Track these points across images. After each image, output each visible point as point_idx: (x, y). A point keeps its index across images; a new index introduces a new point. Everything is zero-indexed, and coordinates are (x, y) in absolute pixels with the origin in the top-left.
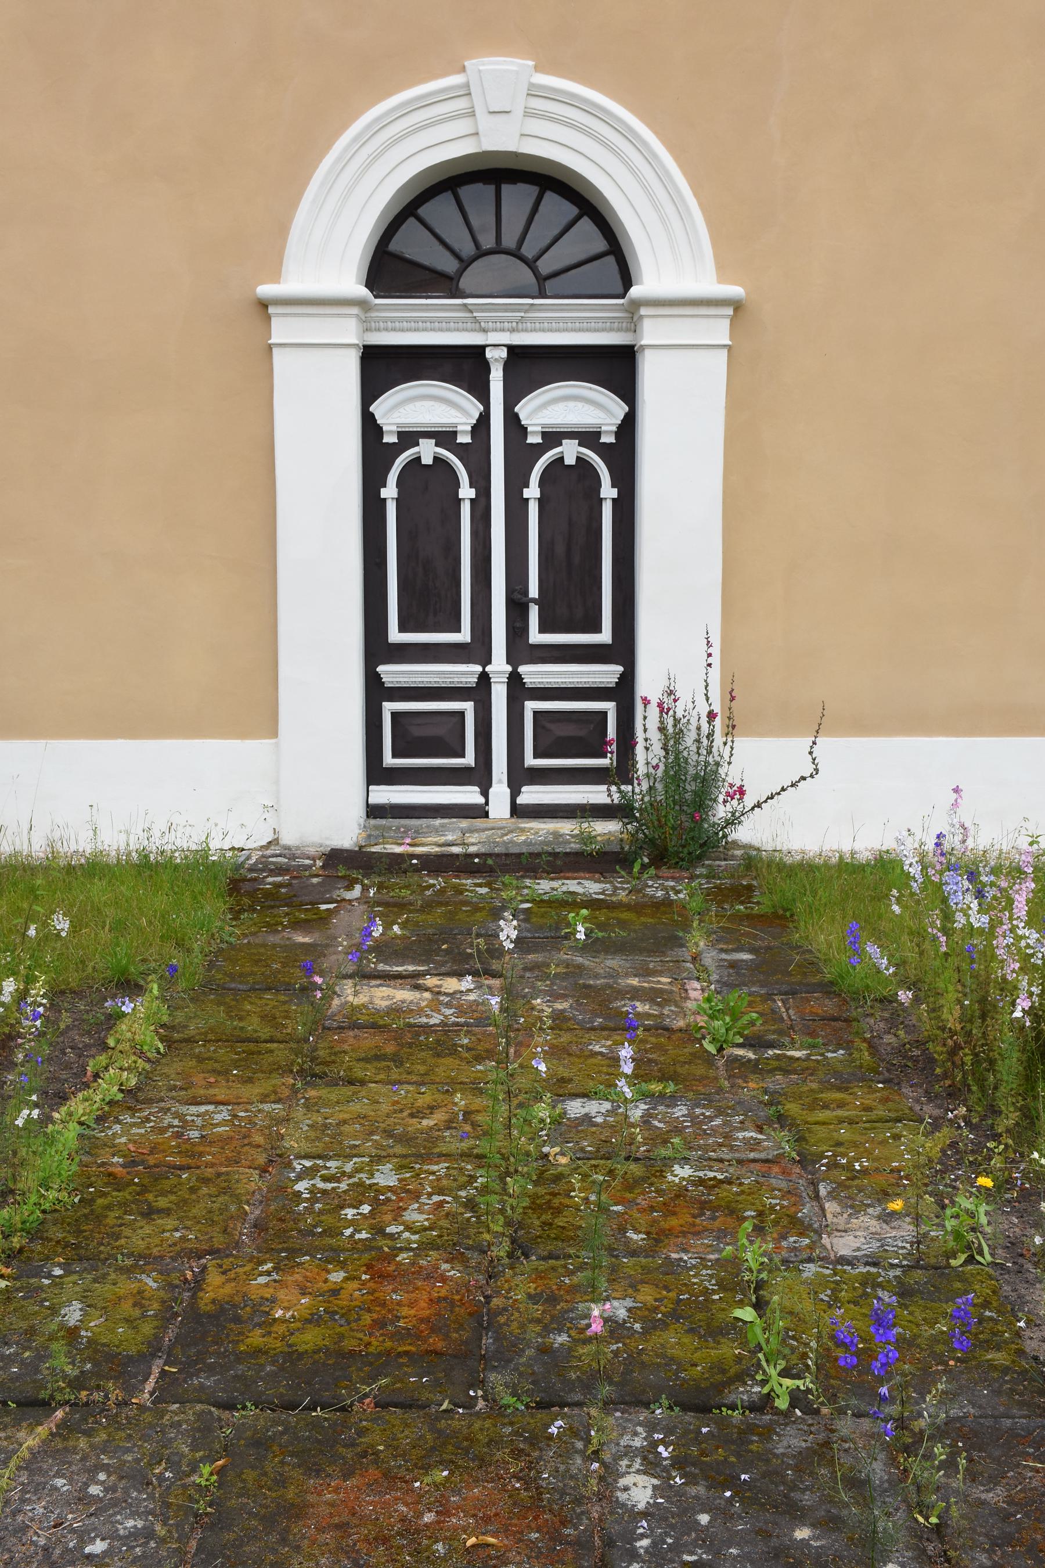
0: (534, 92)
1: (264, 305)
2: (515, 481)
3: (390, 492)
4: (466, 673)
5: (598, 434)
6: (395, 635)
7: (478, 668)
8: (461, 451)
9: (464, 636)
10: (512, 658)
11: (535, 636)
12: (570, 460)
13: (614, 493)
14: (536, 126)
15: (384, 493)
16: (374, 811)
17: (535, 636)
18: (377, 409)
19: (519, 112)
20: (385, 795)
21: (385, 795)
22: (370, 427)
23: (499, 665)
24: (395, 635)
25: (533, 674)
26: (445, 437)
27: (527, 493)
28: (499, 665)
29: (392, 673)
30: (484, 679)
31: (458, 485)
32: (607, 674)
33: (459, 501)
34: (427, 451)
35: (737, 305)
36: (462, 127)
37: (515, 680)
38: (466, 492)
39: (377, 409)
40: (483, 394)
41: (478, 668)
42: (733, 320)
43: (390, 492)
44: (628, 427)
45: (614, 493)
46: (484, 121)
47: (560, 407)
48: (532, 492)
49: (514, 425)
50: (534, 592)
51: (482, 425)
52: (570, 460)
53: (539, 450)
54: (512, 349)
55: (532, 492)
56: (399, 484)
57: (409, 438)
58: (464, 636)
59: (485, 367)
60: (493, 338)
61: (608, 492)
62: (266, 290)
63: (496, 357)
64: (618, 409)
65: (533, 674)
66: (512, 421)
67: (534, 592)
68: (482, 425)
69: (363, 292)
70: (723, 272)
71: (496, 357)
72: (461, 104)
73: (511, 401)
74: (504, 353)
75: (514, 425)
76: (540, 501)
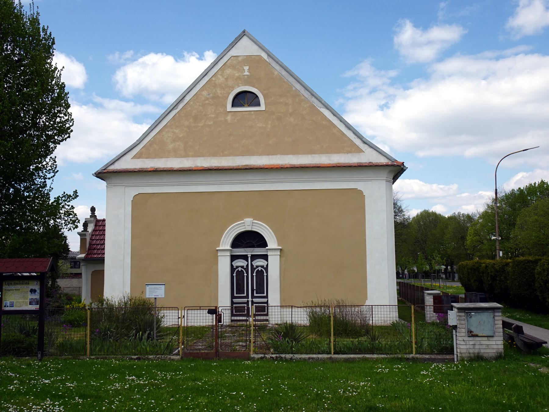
0: (253, 223)
1: (217, 250)
2: (252, 273)
3: (235, 275)
4: (245, 300)
5: (264, 266)
6: (235, 295)
7: (247, 300)
8: (244, 269)
9: (245, 295)
10: (252, 298)
11: (255, 295)
12: (260, 270)
13: (246, 275)
14: (253, 227)
15: (234, 275)
16: (232, 321)
17: (255, 295)
18: (233, 263)
19: (251, 225)
20: (233, 318)
21: (233, 318)
22: (232, 266)
23: (250, 299)
24: (235, 295)
25: (255, 300)
26: (242, 267)
27: (234, 275)
28: (250, 299)
29: (235, 300)
30: (248, 301)
31: (264, 273)
32: (265, 300)
33: (244, 276)
34: (240, 269)
35: (281, 250)
36: (244, 227)
37: (252, 301)
38: (245, 275)
39: (233, 263)
40: (248, 261)
41: (247, 300)
42: (280, 251)
43: (235, 275)
44: (267, 265)
45: (266, 274)
46: (246, 227)
47: (258, 263)
48: (254, 274)
49: (252, 265)
50: (255, 288)
51: (248, 265)
52: (260, 270)
53: (255, 268)
54: (251, 255)
55: (254, 274)
56: (256, 273)
57: (237, 267)
58: (245, 295)
59: (248, 257)
60: (248, 254)
61: (265, 274)
62: (218, 248)
63: (249, 256)
64: (266, 263)
65: (255, 300)
66: (252, 264)
67: (255, 288)
68: (248, 265)
69: (230, 248)
70: (279, 245)
71: (249, 256)
72: (244, 224)
73: (251, 261)
74: (250, 255)
75: (252, 265)
76: (256, 276)
